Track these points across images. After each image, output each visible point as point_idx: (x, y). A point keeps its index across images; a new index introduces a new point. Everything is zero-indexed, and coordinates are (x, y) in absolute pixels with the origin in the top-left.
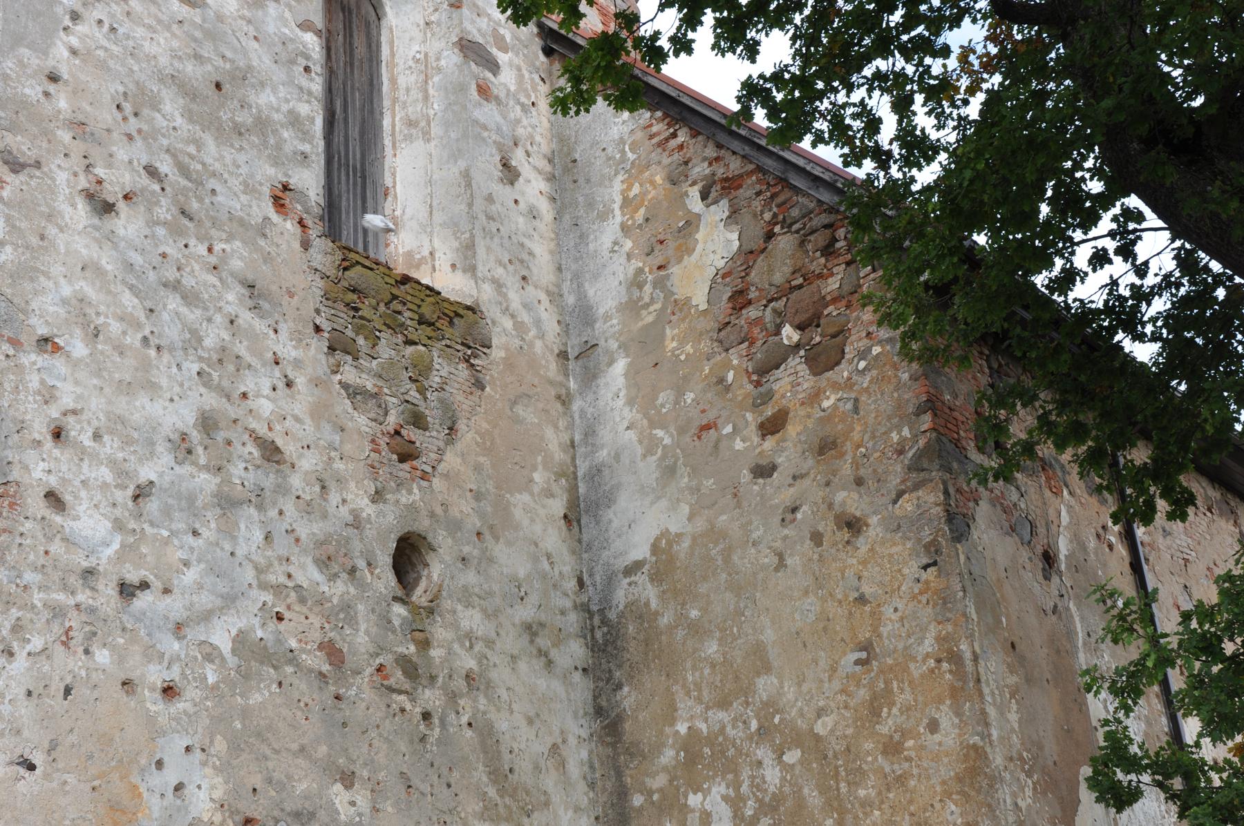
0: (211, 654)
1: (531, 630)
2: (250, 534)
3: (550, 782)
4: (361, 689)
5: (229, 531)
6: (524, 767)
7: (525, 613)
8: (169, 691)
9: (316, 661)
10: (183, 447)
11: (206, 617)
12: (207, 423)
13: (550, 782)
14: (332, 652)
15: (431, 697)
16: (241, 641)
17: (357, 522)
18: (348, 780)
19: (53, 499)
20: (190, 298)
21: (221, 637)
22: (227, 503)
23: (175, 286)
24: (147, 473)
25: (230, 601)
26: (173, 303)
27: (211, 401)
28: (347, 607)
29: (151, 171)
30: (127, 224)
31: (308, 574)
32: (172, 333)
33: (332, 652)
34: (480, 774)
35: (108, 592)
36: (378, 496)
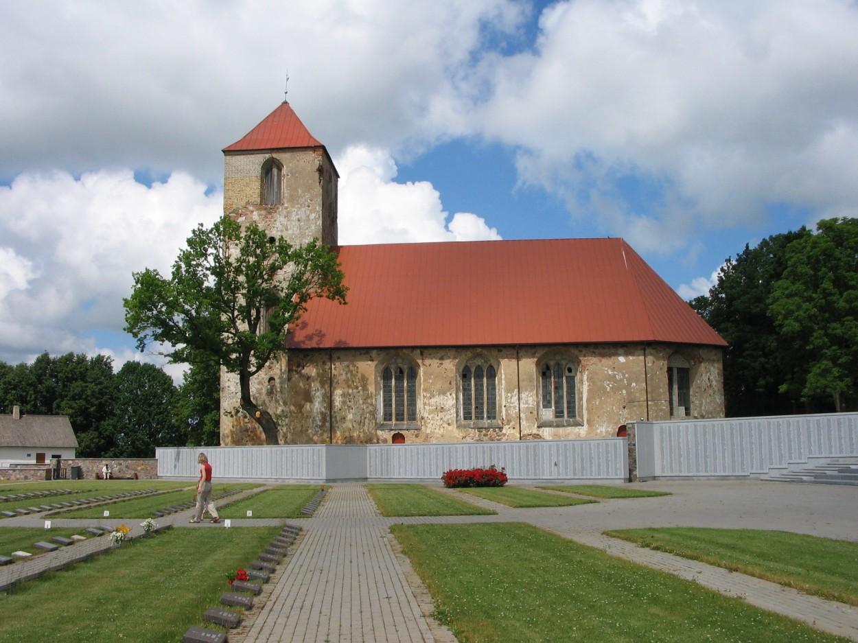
19: (229, 387)
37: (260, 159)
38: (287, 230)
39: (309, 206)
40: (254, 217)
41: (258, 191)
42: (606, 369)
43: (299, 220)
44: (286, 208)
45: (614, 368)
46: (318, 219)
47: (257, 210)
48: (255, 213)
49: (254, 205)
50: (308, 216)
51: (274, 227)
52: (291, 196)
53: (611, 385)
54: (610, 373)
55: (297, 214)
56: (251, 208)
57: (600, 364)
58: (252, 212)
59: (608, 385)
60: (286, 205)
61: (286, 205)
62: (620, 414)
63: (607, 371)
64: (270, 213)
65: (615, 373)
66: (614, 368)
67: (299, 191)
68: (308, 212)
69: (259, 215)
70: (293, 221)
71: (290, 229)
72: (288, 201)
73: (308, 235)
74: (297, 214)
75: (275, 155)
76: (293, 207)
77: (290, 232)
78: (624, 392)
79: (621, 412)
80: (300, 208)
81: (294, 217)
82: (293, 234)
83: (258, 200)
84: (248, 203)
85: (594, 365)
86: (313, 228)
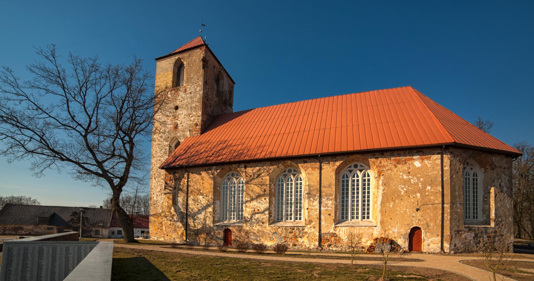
0: (161, 203)
5: (161, 196)
10: (159, 192)
11: (160, 201)
12: (160, 189)
20: (159, 182)
22: (161, 194)
23: (159, 182)
24: (157, 194)
26: (159, 183)
27: (161, 188)
29: (158, 175)
30: (156, 179)
32: (159, 185)
39: (196, 83)
42: (401, 174)
43: (191, 93)
44: (185, 87)
45: (409, 173)
46: (201, 90)
51: (178, 100)
52: (188, 79)
53: (405, 189)
54: (405, 177)
55: (190, 89)
57: (395, 170)
59: (402, 188)
60: (185, 85)
61: (185, 85)
62: (413, 217)
63: (402, 176)
65: (410, 177)
66: (409, 173)
68: (196, 87)
70: (188, 94)
71: (186, 99)
72: (187, 82)
73: (195, 101)
74: (190, 89)
76: (188, 85)
77: (186, 101)
78: (418, 195)
79: (414, 215)
80: (192, 85)
81: (188, 91)
82: (187, 102)
85: (389, 171)
86: (198, 96)
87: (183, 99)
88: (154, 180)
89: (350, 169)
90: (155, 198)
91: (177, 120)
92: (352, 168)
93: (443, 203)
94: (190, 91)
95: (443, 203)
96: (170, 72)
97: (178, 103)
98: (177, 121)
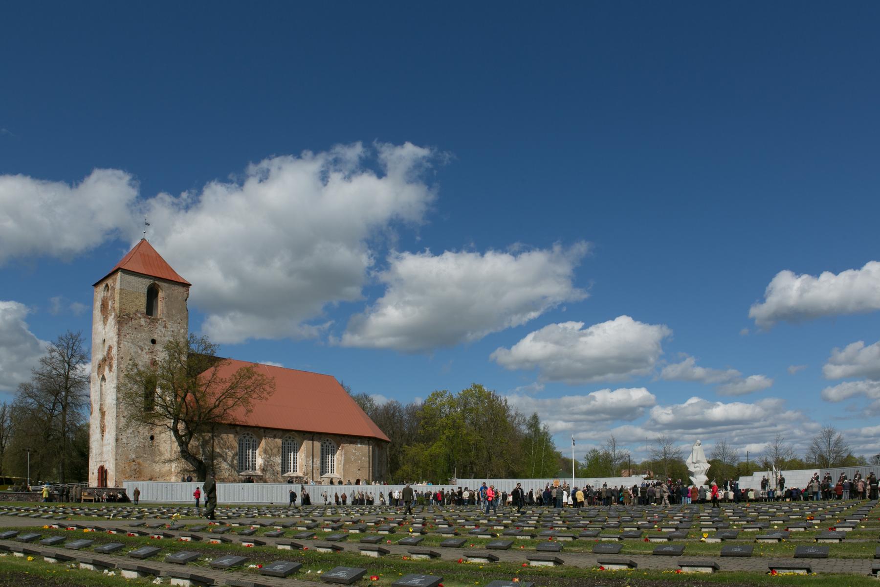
0: (134, 447)
1: (164, 441)
2: (137, 438)
3: (166, 452)
4: (147, 448)
6: (163, 452)
7: (164, 440)
8: (131, 450)
9: (143, 446)
10: (131, 433)
12: (133, 431)
13: (166, 452)
14: (144, 446)
15: (154, 448)
16: (136, 446)
17: (147, 435)
18: (145, 454)
19: (121, 439)
21: (135, 446)
22: (135, 437)
25: (135, 444)
28: (145, 442)
31: (142, 440)
33: (144, 446)
34: (158, 452)
35: (125, 445)
36: (149, 433)
37: (148, 282)
38: (164, 336)
39: (180, 324)
40: (141, 322)
41: (145, 304)
43: (173, 332)
44: (165, 321)
47: (144, 317)
48: (142, 319)
49: (141, 314)
50: (179, 330)
51: (155, 333)
56: (139, 315)
58: (141, 318)
64: (153, 322)
67: (174, 311)
68: (179, 327)
69: (145, 322)
71: (167, 336)
75: (157, 282)
76: (169, 321)
83: (145, 311)
84: (137, 311)
87: (163, 335)
88: (122, 418)
89: (244, 436)
90: (124, 440)
91: (155, 356)
92: (246, 435)
93: (369, 467)
94: (172, 329)
95: (369, 467)
96: (142, 295)
97: (155, 337)
98: (155, 357)
